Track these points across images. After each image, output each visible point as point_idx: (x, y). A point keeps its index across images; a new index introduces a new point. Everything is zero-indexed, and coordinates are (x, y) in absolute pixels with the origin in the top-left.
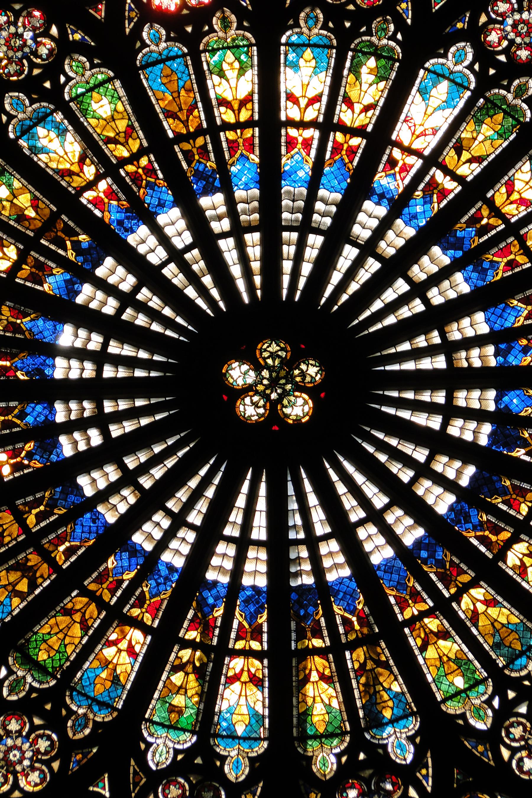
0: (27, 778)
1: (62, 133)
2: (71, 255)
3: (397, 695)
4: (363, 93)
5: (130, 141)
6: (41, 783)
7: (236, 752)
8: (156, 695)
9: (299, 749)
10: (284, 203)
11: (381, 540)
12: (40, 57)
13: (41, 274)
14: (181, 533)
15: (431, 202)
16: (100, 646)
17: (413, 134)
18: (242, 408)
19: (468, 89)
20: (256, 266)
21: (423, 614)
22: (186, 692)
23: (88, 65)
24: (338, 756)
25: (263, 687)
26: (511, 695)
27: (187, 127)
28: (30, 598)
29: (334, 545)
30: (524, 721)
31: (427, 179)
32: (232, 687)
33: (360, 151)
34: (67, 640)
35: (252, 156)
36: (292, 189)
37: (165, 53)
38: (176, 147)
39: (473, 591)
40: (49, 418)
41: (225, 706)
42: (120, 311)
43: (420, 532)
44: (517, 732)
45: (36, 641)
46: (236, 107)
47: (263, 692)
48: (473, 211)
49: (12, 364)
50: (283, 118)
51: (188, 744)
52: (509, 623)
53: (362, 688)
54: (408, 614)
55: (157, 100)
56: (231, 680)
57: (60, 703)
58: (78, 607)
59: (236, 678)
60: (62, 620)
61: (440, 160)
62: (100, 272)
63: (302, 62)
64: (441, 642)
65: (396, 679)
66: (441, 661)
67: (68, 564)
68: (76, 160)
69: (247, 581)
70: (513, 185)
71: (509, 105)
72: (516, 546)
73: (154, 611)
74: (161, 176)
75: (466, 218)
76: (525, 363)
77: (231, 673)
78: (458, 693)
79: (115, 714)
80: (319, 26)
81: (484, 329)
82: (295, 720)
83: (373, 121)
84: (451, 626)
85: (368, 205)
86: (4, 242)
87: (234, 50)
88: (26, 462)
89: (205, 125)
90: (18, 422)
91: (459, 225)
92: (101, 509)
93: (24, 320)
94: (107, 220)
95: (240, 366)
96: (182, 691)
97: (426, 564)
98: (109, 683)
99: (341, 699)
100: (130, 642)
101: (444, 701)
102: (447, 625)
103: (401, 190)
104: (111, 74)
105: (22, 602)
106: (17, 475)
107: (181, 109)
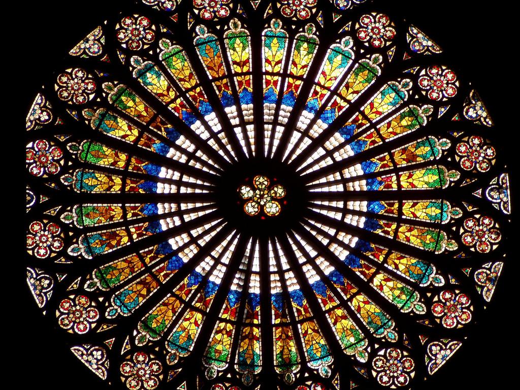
1: (159, 76)
2: (164, 134)
3: (323, 346)
5: (191, 80)
6: (154, 386)
10: (265, 111)
11: (314, 272)
12: (148, 40)
15: (335, 112)
16: (181, 321)
17: (326, 79)
18: (247, 208)
19: (351, 58)
20: (252, 141)
21: (334, 308)
22: (223, 343)
23: (170, 44)
26: (377, 346)
27: (218, 74)
28: (147, 298)
33: (301, 87)
36: (268, 104)
37: (207, 39)
38: (213, 83)
39: (357, 297)
42: (188, 161)
44: (380, 364)
45: (151, 318)
50: (264, 71)
51: (224, 368)
52: (375, 312)
53: (306, 342)
54: (327, 307)
55: (204, 61)
56: (243, 339)
57: (163, 348)
58: (170, 302)
59: (246, 337)
61: (338, 92)
62: (178, 142)
63: (272, 45)
67: (165, 281)
72: (377, 276)
74: (206, 97)
75: (351, 120)
76: (381, 189)
77: (244, 335)
78: (351, 345)
79: (189, 353)
81: (361, 173)
83: (307, 73)
85: (305, 113)
88: (144, 233)
90: (140, 213)
92: (180, 255)
93: (142, 165)
94: (181, 118)
96: (221, 343)
97: (336, 284)
98: (186, 339)
100: (196, 319)
103: (320, 106)
104: (181, 48)
105: (144, 299)
106: (140, 239)
107: (215, 66)
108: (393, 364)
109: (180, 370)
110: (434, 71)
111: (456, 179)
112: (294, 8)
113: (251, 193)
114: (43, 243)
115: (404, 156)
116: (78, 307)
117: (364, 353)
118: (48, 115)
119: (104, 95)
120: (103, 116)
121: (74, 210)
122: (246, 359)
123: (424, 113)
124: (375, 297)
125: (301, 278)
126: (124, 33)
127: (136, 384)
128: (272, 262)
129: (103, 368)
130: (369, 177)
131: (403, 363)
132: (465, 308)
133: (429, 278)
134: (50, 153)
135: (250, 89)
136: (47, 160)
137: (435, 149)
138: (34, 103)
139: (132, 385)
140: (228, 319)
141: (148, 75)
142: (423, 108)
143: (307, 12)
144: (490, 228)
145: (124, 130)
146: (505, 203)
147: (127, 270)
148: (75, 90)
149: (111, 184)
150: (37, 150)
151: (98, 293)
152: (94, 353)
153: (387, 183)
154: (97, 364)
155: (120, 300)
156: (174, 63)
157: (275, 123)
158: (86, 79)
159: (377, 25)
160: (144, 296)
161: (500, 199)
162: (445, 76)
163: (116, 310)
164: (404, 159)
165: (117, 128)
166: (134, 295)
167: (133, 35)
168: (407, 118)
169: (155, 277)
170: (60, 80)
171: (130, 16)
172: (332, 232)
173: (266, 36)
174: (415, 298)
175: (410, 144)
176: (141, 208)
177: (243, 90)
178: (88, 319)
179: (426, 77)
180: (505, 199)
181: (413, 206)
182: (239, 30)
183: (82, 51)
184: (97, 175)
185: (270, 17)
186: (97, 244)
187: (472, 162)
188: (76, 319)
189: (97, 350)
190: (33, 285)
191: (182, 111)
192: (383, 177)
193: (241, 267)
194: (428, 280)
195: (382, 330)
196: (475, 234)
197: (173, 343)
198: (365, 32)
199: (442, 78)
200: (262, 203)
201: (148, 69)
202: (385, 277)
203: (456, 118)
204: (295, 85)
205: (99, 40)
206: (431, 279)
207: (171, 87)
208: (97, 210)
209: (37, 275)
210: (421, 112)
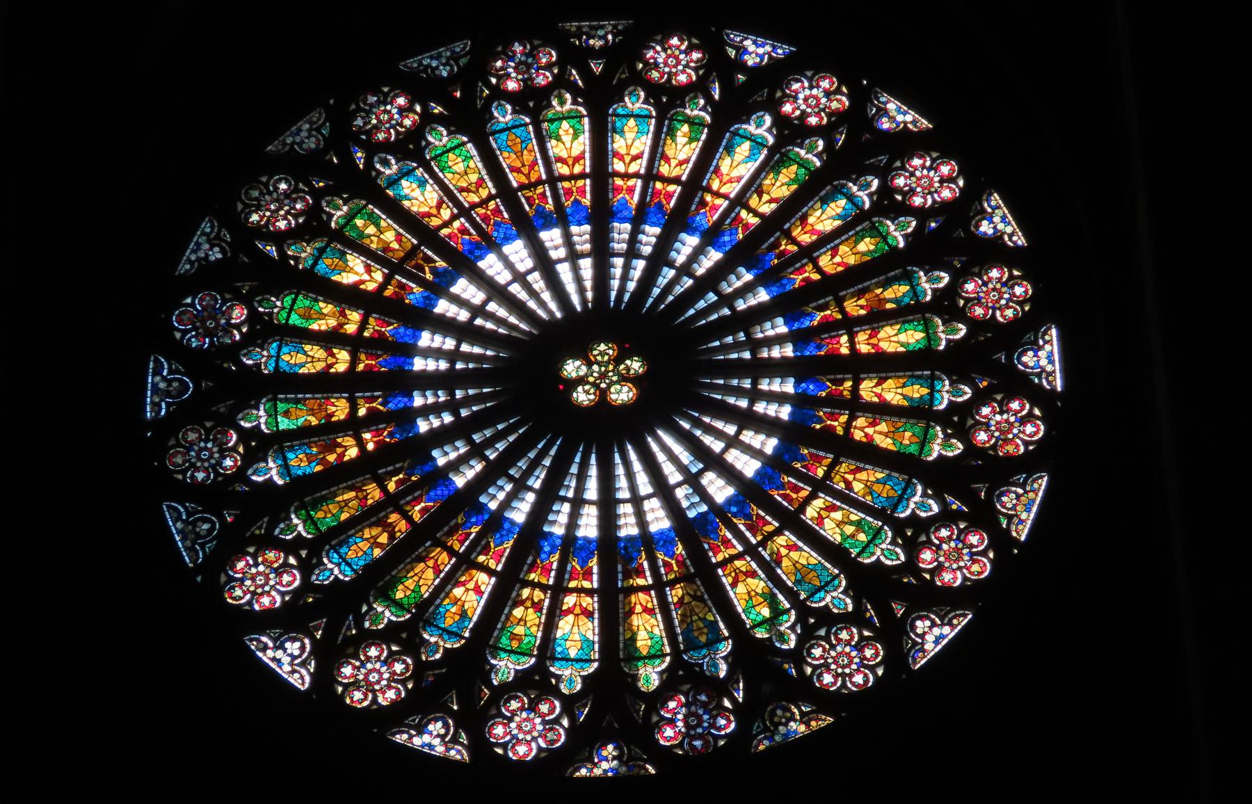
0: (384, 695)
1: (422, 184)
2: (429, 276)
4: (678, 152)
5: (480, 189)
12: (405, 127)
13: (402, 292)
16: (449, 587)
18: (575, 395)
21: (732, 558)
22: (525, 624)
25: (593, 618)
31: (733, 215)
32: (566, 618)
34: (421, 584)
35: (584, 200)
40: (408, 404)
46: (570, 162)
47: (593, 622)
48: (772, 239)
49: (377, 363)
51: (527, 666)
52: (809, 564)
54: (720, 557)
55: (504, 158)
59: (570, 611)
62: (454, 289)
64: (749, 580)
65: (710, 611)
66: (749, 595)
68: (434, 204)
69: (580, 533)
71: (802, 159)
74: (506, 215)
77: (565, 607)
79: (463, 641)
81: (782, 329)
82: (621, 645)
83: (687, 172)
84: (758, 566)
86: (372, 268)
87: (568, 120)
88: (388, 440)
90: (381, 408)
91: (760, 251)
93: (388, 329)
95: (573, 362)
96: (522, 623)
97: (735, 518)
98: (457, 618)
102: (754, 565)
109: (444, 671)
112: (667, 69)
114: (203, 461)
115: (862, 302)
118: (223, 251)
120: (322, 251)
122: (568, 649)
123: (898, 233)
126: (363, 118)
128: (622, 483)
130: (798, 338)
133: (908, 504)
136: (218, 324)
137: (919, 288)
138: (199, 233)
139: (355, 699)
141: (404, 183)
143: (689, 75)
144: (1022, 418)
145: (356, 273)
149: (330, 360)
153: (830, 346)
154: (291, 664)
155: (338, 553)
156: (450, 164)
159: (815, 92)
161: (1041, 367)
163: (332, 570)
164: (862, 307)
165: (346, 269)
166: (365, 544)
168: (867, 240)
170: (246, 196)
172: (731, 429)
174: (883, 538)
175: (873, 281)
177: (572, 203)
178: (278, 587)
183: (287, 148)
184: (307, 348)
186: (301, 460)
187: (987, 308)
188: (256, 588)
194: (907, 507)
195: (822, 594)
200: (603, 385)
202: (827, 504)
204: (667, 191)
205: (318, 130)
206: (912, 505)
207: (444, 202)
209: (189, 514)
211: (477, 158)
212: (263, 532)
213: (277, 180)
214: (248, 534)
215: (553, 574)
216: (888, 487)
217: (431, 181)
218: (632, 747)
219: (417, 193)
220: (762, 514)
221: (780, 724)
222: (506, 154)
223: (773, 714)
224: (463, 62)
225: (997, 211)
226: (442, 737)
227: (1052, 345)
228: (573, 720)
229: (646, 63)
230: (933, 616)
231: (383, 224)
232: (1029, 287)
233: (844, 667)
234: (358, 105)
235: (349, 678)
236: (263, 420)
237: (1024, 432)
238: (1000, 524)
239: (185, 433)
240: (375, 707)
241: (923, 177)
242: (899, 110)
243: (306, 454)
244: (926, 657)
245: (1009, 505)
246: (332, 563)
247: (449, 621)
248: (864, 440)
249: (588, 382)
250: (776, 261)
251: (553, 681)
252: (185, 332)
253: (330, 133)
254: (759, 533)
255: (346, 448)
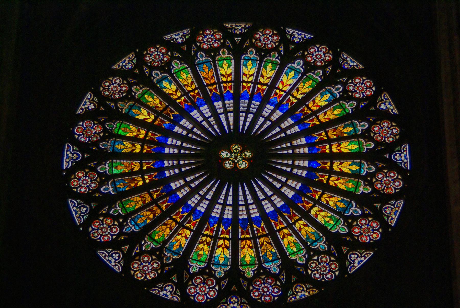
1: (170, 83)
2: (172, 117)
5: (192, 85)
7: (219, 269)
8: (194, 251)
9: (241, 269)
10: (241, 105)
11: (269, 205)
12: (165, 61)
14: (204, 201)
16: (175, 235)
17: (283, 86)
18: (225, 164)
20: (231, 123)
21: (283, 228)
22: (204, 250)
23: (180, 63)
24: (254, 271)
25: (229, 249)
26: (312, 253)
29: (254, 206)
30: (316, 262)
31: (287, 98)
32: (219, 249)
33: (266, 90)
34: (165, 233)
35: (231, 91)
36: (244, 101)
39: (299, 222)
41: (216, 255)
43: (283, 203)
44: (314, 265)
48: (302, 108)
50: (242, 80)
51: (204, 266)
53: (262, 250)
54: (278, 228)
56: (219, 247)
57: (161, 252)
58: (169, 223)
59: (220, 246)
60: (164, 227)
61: (291, 93)
62: (181, 123)
63: (248, 64)
64: (289, 237)
69: (225, 217)
70: (315, 101)
72: (314, 208)
73: (194, 225)
74: (202, 96)
77: (219, 245)
79: (180, 256)
80: (254, 54)
82: (240, 260)
83: (270, 82)
88: (154, 179)
89: (216, 82)
90: (152, 167)
92: (178, 193)
93: (156, 137)
96: (202, 250)
98: (178, 247)
99: (255, 254)
100: (186, 234)
101: (289, 255)
102: (291, 231)
104: (187, 66)
107: (209, 77)
108: (323, 266)
109: (172, 267)
110: (357, 81)
111: (371, 148)
112: (264, 42)
113: (229, 155)
114: (84, 184)
115: (335, 133)
116: (105, 226)
117: (303, 258)
118: (95, 105)
119: (133, 94)
121: (107, 164)
123: (349, 107)
124: (313, 222)
125: (261, 208)
126: (149, 57)
127: (141, 276)
129: (119, 265)
131: (331, 265)
132: (376, 230)
134: (94, 129)
135: (232, 91)
136: (92, 133)
137: (357, 129)
138: (86, 98)
139: (138, 276)
140: (208, 234)
141: (164, 82)
142: (349, 103)
143: (272, 45)
144: (394, 179)
145: (145, 115)
146: (405, 163)
147: (141, 203)
148: (114, 91)
150: (85, 127)
151: (119, 216)
152: (114, 255)
153: (322, 149)
154: (115, 262)
155: (134, 221)
156: (181, 75)
157: (247, 112)
158: (121, 84)
159: (320, 53)
160: (150, 219)
161: (402, 160)
162: (365, 84)
163: (131, 227)
164: (335, 135)
165: (141, 114)
166: (144, 218)
167: (155, 58)
168: (337, 110)
169: (159, 207)
171: (154, 47)
172: (284, 179)
173: (244, 59)
174: (340, 223)
175: (339, 125)
176: (153, 164)
178: (111, 233)
179: (352, 85)
180: (405, 161)
181: (340, 165)
182: (226, 55)
183: (120, 67)
185: (248, 48)
186: (121, 185)
187: (382, 137)
189: (116, 253)
190: (74, 211)
191: (185, 104)
192: (320, 146)
193: (219, 201)
194: (350, 211)
195: (316, 243)
196: (383, 183)
197: (169, 250)
198: (311, 57)
199: (363, 85)
200: (236, 161)
201: (164, 78)
202: (319, 209)
203: (373, 108)
205: (132, 61)
208: (123, 164)
209: (78, 204)
210: (347, 106)
211: (191, 74)
212: (106, 212)
213: (116, 79)
214: (100, 213)
215: (215, 232)
216: (342, 204)
217: (174, 82)
218: (242, 299)
219: (168, 86)
220: (295, 212)
221: (299, 292)
222: (202, 73)
223: (296, 288)
224: (187, 37)
225: (387, 101)
226: (171, 292)
227: (407, 152)
228: (220, 287)
229: (256, 40)
230: (358, 253)
231: (155, 97)
232: (398, 130)
233: (323, 271)
234: (147, 52)
235: (137, 268)
236: (107, 170)
237: (395, 185)
238: (384, 219)
239: (78, 174)
240: (146, 280)
241: (360, 86)
242: (351, 61)
243: (123, 183)
244: (354, 268)
245: (388, 212)
246: (132, 225)
247: (175, 248)
248: (334, 185)
249: (230, 160)
250: (303, 117)
251: (213, 272)
252: (79, 135)
253: (136, 63)
254: (293, 219)
255: (138, 181)
